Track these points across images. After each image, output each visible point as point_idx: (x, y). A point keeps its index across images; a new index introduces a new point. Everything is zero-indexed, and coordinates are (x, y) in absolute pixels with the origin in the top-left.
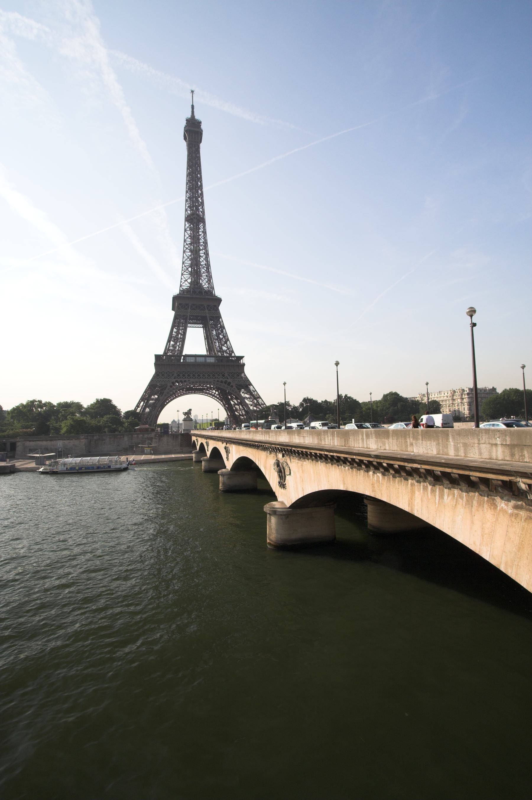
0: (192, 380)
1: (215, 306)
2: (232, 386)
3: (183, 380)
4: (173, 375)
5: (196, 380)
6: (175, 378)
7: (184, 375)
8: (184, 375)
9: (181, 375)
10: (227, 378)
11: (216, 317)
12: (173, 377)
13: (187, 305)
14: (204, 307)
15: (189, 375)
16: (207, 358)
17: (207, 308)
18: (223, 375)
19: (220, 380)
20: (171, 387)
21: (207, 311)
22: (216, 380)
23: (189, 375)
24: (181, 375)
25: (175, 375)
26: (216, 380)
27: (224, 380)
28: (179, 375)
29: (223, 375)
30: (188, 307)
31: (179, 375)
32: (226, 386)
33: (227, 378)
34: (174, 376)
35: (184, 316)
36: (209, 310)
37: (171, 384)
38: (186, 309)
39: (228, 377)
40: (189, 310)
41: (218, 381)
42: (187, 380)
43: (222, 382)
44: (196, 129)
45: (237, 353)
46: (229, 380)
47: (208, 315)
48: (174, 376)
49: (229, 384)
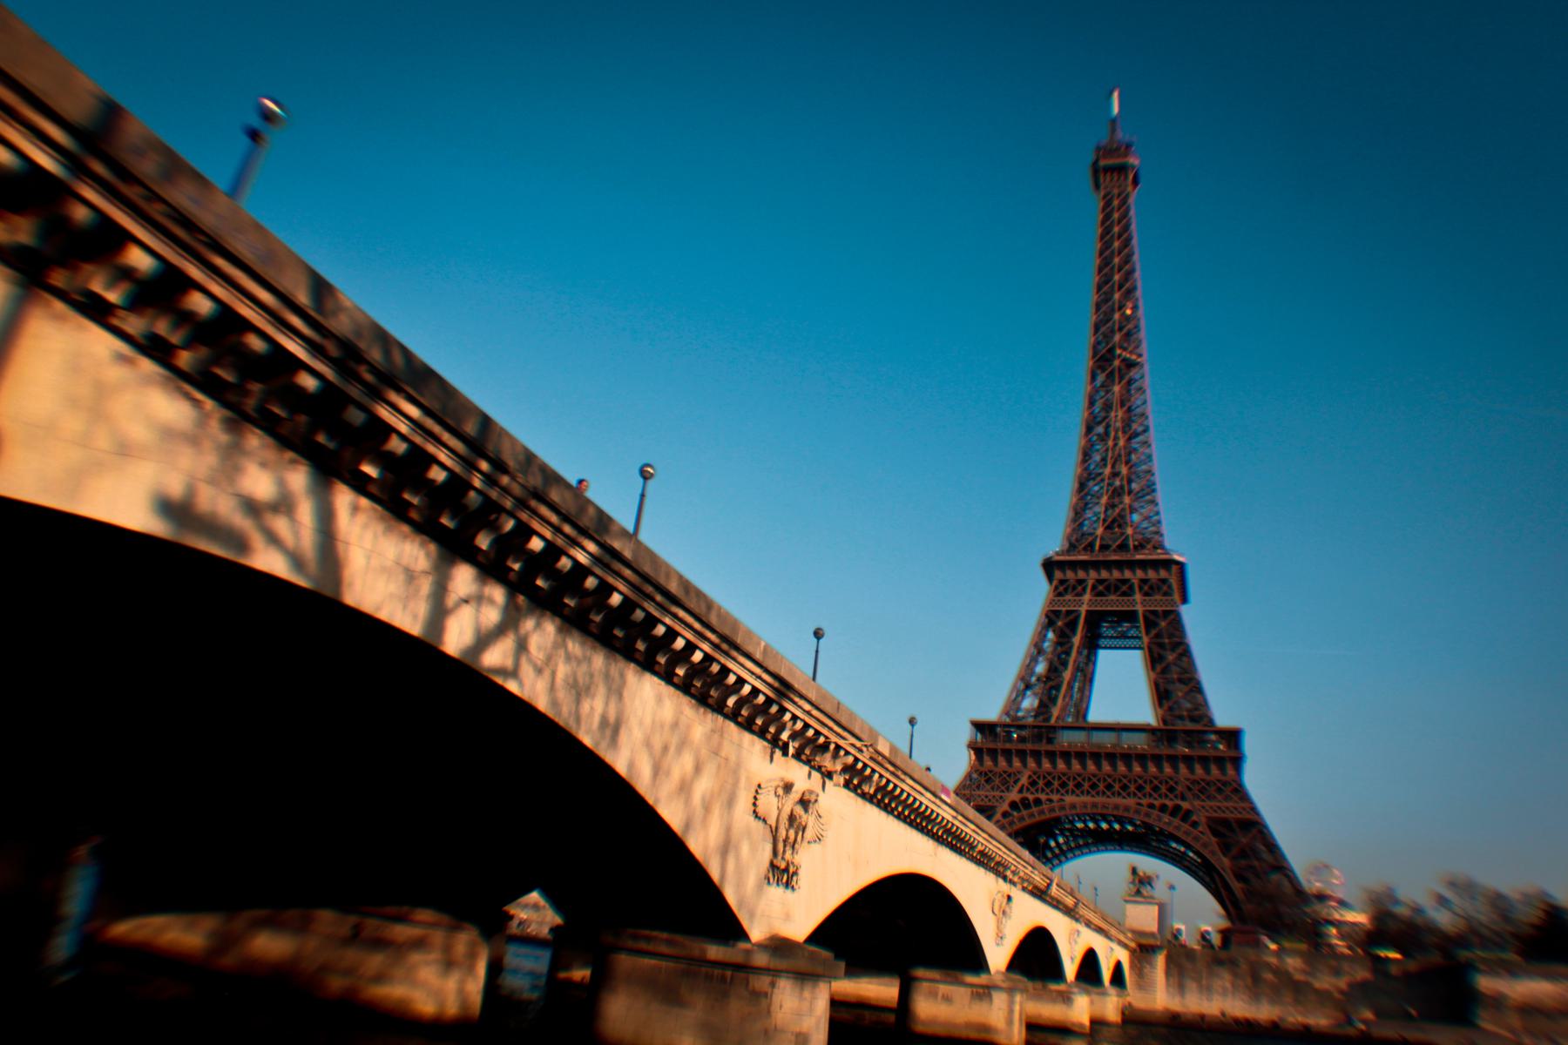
0: (1069, 799)
1: (1164, 581)
2: (1194, 824)
3: (1043, 797)
6: (1020, 791)
7: (1048, 784)
10: (1183, 798)
11: (1166, 613)
12: (1017, 787)
13: (1080, 582)
14: (1131, 588)
15: (1063, 785)
16: (1125, 735)
17: (1140, 588)
18: (1171, 789)
21: (1138, 597)
22: (1144, 801)
23: (1063, 785)
24: (1041, 783)
25: (1024, 780)
28: (1033, 783)
29: (1171, 789)
30: (1084, 589)
32: (1176, 821)
34: (1017, 787)
35: (1069, 613)
36: (1146, 594)
38: (1079, 595)
40: (1087, 597)
42: (1055, 797)
43: (1163, 808)
45: (1222, 719)
46: (1185, 805)
47: (1140, 609)
49: (1188, 813)
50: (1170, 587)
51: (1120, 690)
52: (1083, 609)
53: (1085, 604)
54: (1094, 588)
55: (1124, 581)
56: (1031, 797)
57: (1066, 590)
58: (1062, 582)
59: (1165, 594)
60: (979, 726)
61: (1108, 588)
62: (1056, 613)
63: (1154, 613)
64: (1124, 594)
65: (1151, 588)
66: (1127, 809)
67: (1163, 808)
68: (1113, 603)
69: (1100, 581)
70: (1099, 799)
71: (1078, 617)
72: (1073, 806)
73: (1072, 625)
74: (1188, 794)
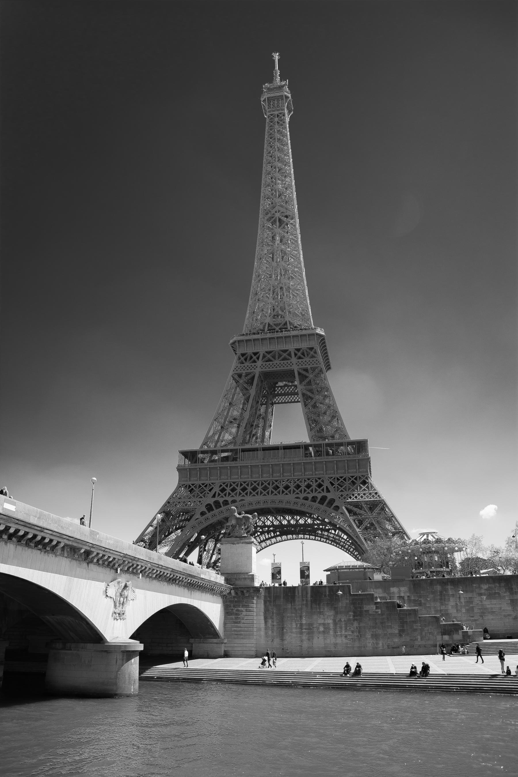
1: (311, 349)
3: (230, 499)
4: (210, 490)
5: (260, 498)
6: (214, 496)
8: (233, 490)
9: (228, 490)
10: (328, 491)
11: (313, 369)
13: (255, 354)
14: (290, 355)
15: (244, 489)
17: (296, 355)
18: (320, 486)
19: (310, 496)
20: (203, 514)
21: (294, 360)
22: (302, 496)
23: (244, 489)
25: (217, 489)
26: (302, 496)
27: (319, 496)
28: (223, 490)
29: (320, 486)
30: (258, 358)
31: (223, 490)
33: (328, 491)
35: (247, 375)
36: (300, 358)
37: (204, 509)
38: (254, 362)
39: (331, 488)
40: (259, 363)
41: (306, 499)
42: (238, 498)
44: (281, 94)
45: (354, 436)
46: (330, 496)
47: (296, 369)
48: (213, 492)
49: (332, 501)
50: (315, 352)
51: (288, 426)
52: (257, 372)
53: (259, 368)
54: (264, 356)
55: (285, 351)
56: (221, 500)
57: (246, 360)
58: (243, 355)
59: (313, 357)
60: (186, 454)
61: (274, 357)
62: (240, 376)
63: (306, 370)
64: (285, 359)
65: (303, 354)
66: (288, 502)
67: (314, 499)
68: (277, 366)
69: (269, 353)
70: (270, 497)
71: (253, 377)
72: (251, 504)
73: (251, 382)
74: (331, 488)
